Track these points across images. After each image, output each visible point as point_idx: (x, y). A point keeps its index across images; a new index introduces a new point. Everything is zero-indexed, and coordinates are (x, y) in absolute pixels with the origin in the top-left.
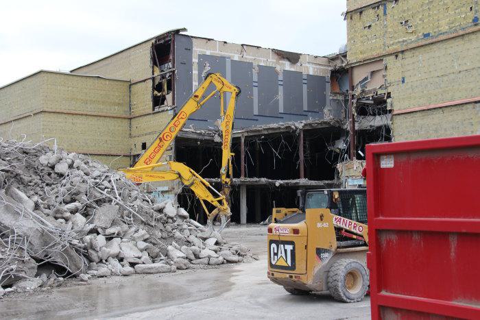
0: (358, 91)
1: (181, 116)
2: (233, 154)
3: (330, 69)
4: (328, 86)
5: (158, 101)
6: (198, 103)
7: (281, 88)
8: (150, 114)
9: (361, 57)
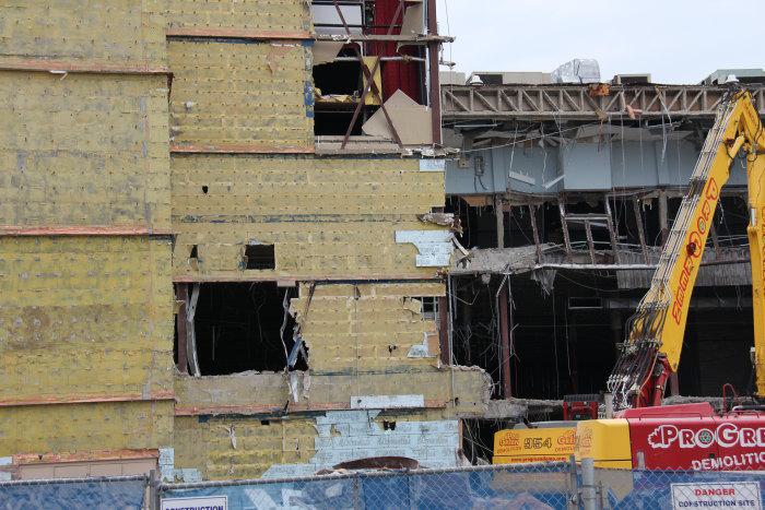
5: (330, 121)
8: (304, 156)
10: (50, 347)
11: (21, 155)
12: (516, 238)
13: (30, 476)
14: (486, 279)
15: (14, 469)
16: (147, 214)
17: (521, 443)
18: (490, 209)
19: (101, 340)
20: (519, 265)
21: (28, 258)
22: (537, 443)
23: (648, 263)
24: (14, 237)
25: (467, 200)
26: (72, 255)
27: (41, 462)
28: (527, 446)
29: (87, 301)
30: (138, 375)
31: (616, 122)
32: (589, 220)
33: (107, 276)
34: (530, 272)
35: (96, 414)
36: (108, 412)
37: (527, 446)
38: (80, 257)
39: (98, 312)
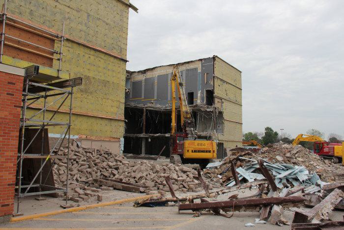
10: (91, 93)
11: (89, 15)
13: (85, 145)
15: (80, 140)
16: (121, 52)
17: (196, 144)
19: (106, 95)
21: (87, 56)
22: (201, 145)
24: (84, 46)
26: (100, 59)
27: (87, 139)
28: (198, 145)
29: (103, 78)
30: (115, 110)
33: (109, 70)
35: (103, 122)
36: (106, 122)
37: (198, 145)
38: (102, 61)
39: (105, 83)
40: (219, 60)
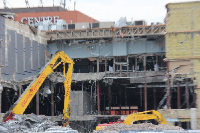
0: (173, 74)
1: (43, 76)
2: (71, 101)
3: (46, 39)
4: (45, 50)
6: (52, 68)
7: (31, 52)
9: (176, 57)
12: (102, 69)
14: (90, 82)
18: (96, 61)
20: (99, 78)
23: (136, 76)
25: (89, 59)
31: (118, 37)
32: (121, 64)
34: (103, 80)
40: (176, 6)
